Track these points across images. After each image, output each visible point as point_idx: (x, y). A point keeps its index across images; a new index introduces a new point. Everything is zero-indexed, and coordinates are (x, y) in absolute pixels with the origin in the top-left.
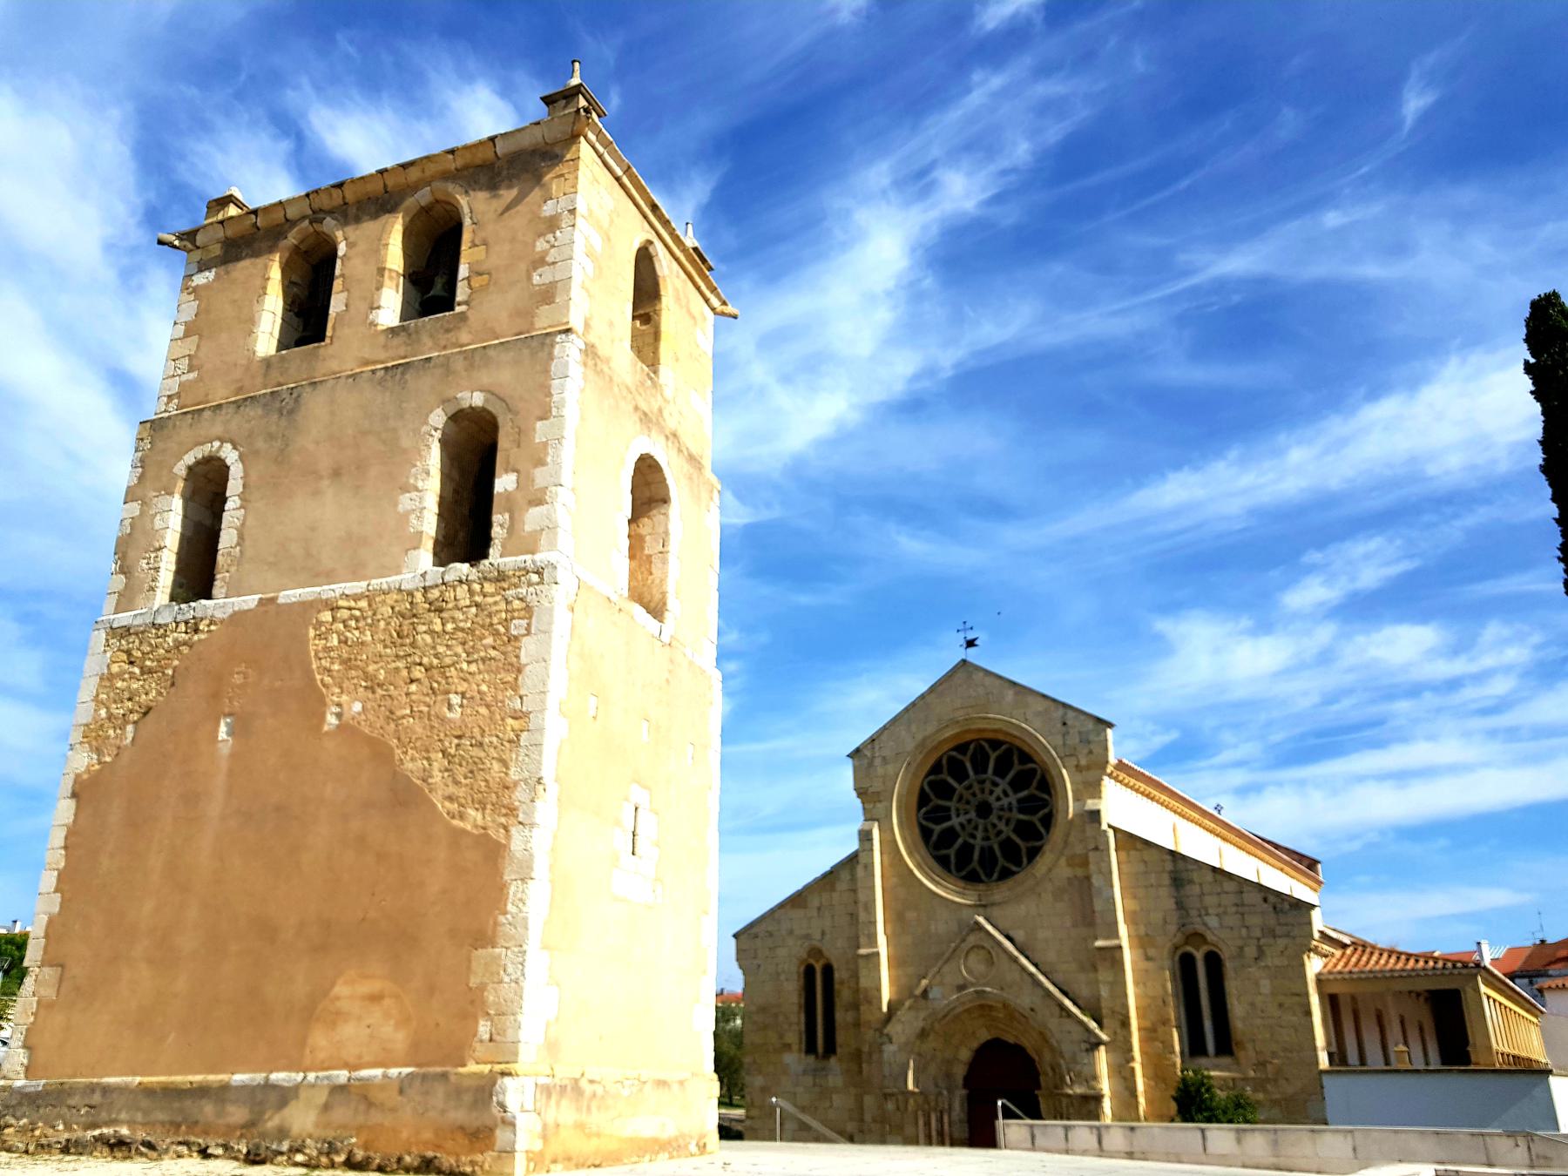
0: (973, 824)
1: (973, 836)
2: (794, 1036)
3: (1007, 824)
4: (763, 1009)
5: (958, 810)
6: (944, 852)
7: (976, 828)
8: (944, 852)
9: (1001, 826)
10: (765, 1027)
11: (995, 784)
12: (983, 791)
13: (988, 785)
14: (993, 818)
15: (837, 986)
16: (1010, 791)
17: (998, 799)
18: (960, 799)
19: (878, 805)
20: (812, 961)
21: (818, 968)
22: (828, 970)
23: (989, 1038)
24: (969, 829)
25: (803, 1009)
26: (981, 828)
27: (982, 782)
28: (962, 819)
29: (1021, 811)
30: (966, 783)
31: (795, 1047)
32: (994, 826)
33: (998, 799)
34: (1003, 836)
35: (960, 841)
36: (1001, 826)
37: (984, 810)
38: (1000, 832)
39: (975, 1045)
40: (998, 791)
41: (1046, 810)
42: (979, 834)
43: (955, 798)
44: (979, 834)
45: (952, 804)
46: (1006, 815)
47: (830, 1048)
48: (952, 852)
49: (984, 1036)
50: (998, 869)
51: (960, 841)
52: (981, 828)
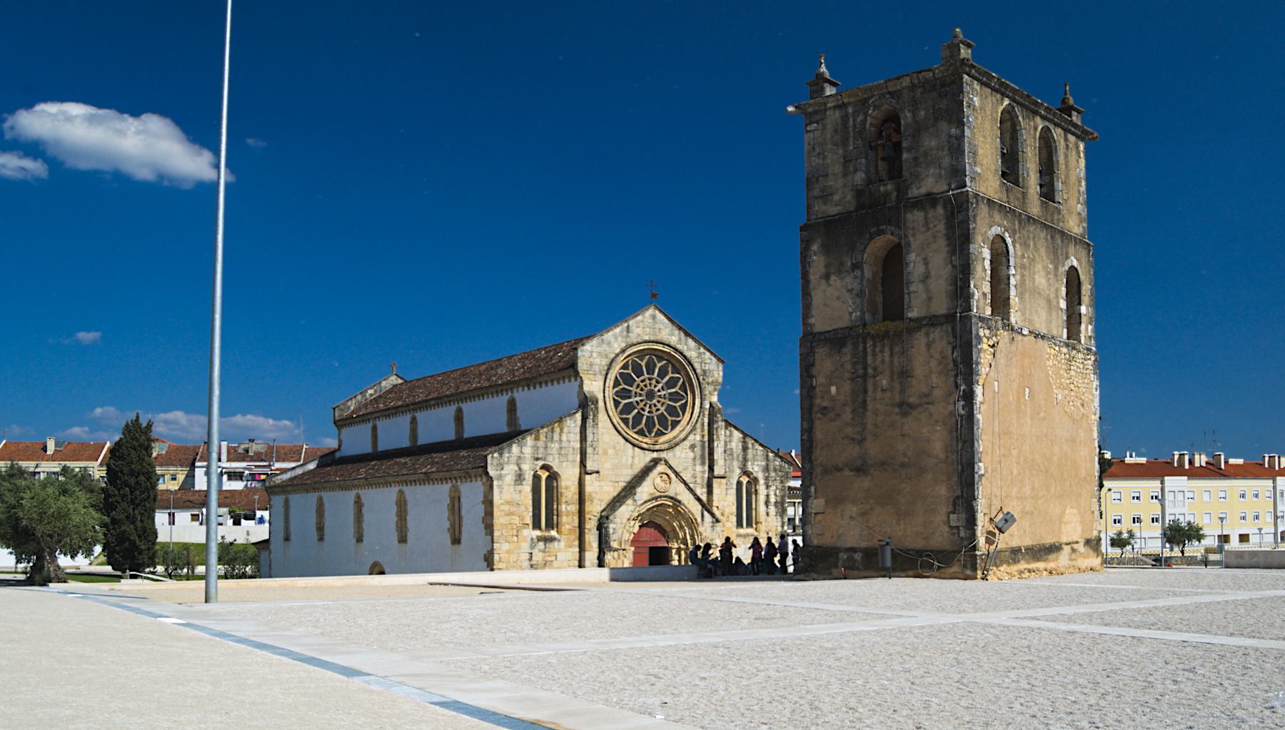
0: (644, 403)
1: (643, 410)
2: (529, 520)
3: (662, 406)
4: (509, 503)
5: (636, 393)
6: (624, 416)
7: (645, 405)
8: (624, 416)
9: (659, 406)
10: (510, 514)
11: (658, 382)
12: (650, 384)
13: (654, 382)
14: (655, 401)
16: (665, 388)
17: (659, 391)
18: (638, 386)
19: (594, 383)
24: (642, 405)
26: (648, 406)
27: (650, 379)
28: (638, 399)
29: (670, 400)
30: (642, 378)
31: (531, 526)
32: (655, 406)
33: (659, 391)
34: (659, 412)
35: (636, 411)
36: (659, 406)
37: (650, 395)
38: (658, 410)
40: (659, 386)
41: (683, 402)
42: (647, 409)
43: (635, 386)
44: (647, 409)
45: (633, 389)
46: (662, 400)
48: (630, 416)
50: (655, 430)
51: (636, 411)
52: (648, 406)
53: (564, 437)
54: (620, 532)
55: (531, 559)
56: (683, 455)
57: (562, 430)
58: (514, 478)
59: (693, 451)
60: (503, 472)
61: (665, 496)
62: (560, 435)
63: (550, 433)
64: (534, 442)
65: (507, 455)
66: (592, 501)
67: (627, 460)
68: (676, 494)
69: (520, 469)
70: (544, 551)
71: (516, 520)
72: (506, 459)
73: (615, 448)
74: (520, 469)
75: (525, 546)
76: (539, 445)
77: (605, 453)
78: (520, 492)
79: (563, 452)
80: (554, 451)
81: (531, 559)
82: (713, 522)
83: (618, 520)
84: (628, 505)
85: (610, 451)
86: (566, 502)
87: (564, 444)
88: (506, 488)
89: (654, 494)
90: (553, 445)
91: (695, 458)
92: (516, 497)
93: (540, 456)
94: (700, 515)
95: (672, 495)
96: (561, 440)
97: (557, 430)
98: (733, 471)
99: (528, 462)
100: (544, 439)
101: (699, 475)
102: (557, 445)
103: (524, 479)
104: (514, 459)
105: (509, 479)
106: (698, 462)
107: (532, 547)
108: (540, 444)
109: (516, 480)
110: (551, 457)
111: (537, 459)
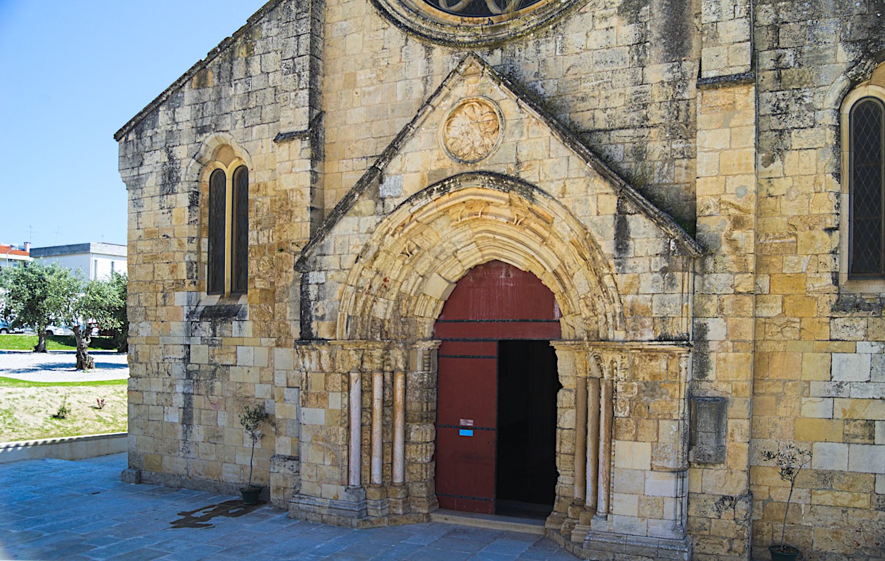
4: (150, 235)
15: (251, 196)
20: (219, 165)
21: (229, 173)
22: (242, 174)
23: (479, 261)
25: (205, 234)
39: (456, 272)
47: (241, 285)
49: (473, 258)
53: (255, 68)
54: (337, 296)
55: (187, 359)
56: (597, 39)
57: (250, 51)
58: (160, 181)
59: (635, 19)
60: (143, 170)
61: (474, 175)
62: (247, 63)
63: (227, 65)
64: (195, 93)
65: (149, 133)
66: (291, 213)
67: (409, 90)
68: (518, 163)
69: (170, 158)
70: (211, 343)
71: (163, 271)
72: (148, 142)
73: (375, 63)
74: (170, 158)
75: (178, 327)
76: (206, 98)
77: (351, 82)
78: (170, 209)
79: (253, 104)
80: (235, 105)
81: (187, 359)
82: (667, 254)
83: (331, 261)
84: (359, 214)
85: (362, 76)
86: (258, 223)
87: (256, 83)
88: (146, 202)
89: (442, 170)
90: (232, 91)
91: (641, 42)
92: (164, 220)
93: (207, 122)
94: (612, 232)
95: (503, 170)
96: (248, 75)
97: (242, 53)
98: (819, 59)
99: (185, 141)
100: (216, 81)
101: (656, 94)
102: (241, 89)
103: (178, 178)
104: (161, 138)
105: (152, 183)
106: (655, 52)
107: (189, 334)
108: (209, 93)
109: (164, 185)
110: (228, 119)
111: (202, 130)
